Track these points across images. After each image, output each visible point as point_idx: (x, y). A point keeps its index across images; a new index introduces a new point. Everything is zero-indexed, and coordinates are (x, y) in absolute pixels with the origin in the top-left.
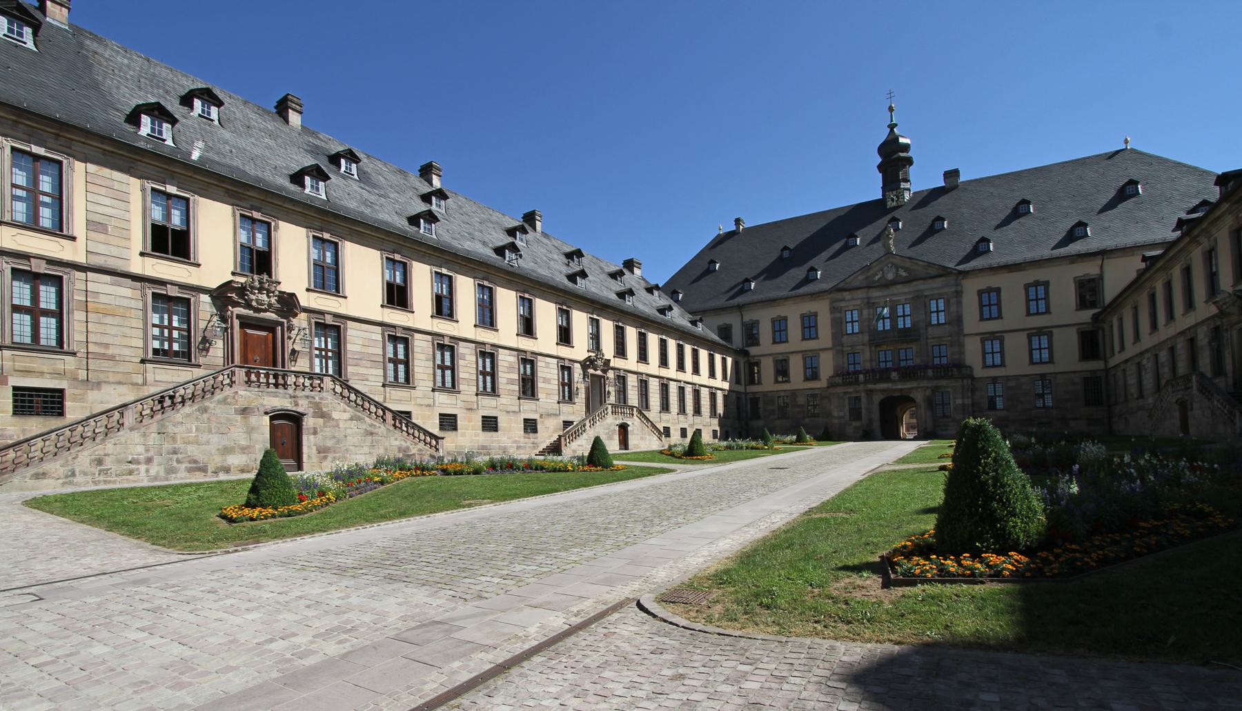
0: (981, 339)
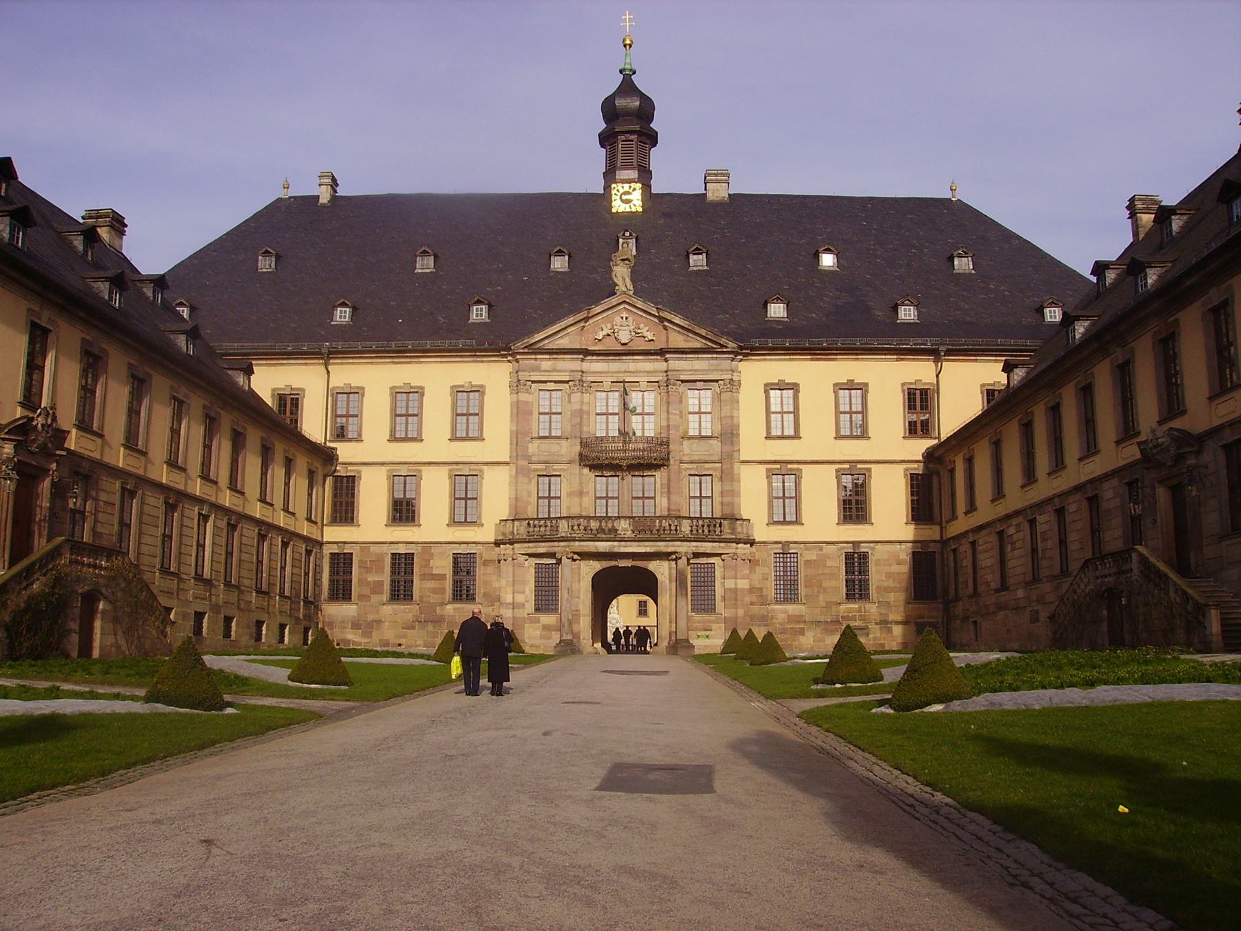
0: (768, 470)
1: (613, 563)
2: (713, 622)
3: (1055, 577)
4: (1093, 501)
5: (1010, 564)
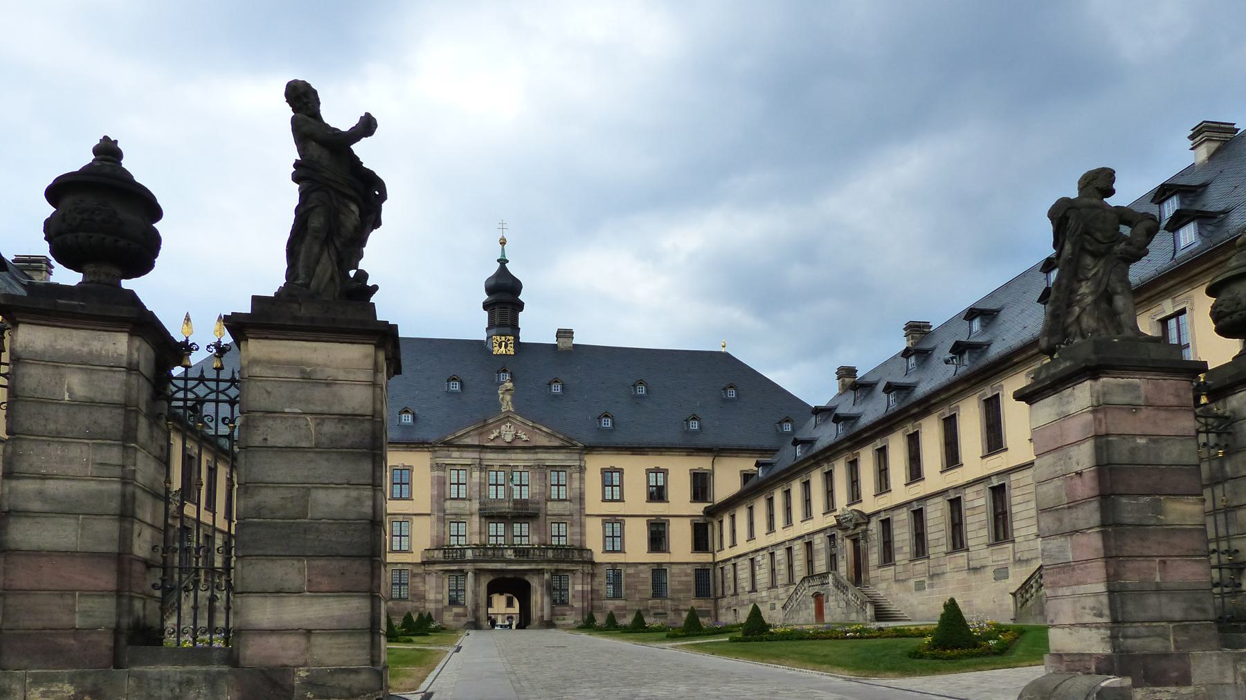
1: (501, 576)
2: (568, 610)
3: (785, 585)
4: (809, 545)
5: (758, 577)
